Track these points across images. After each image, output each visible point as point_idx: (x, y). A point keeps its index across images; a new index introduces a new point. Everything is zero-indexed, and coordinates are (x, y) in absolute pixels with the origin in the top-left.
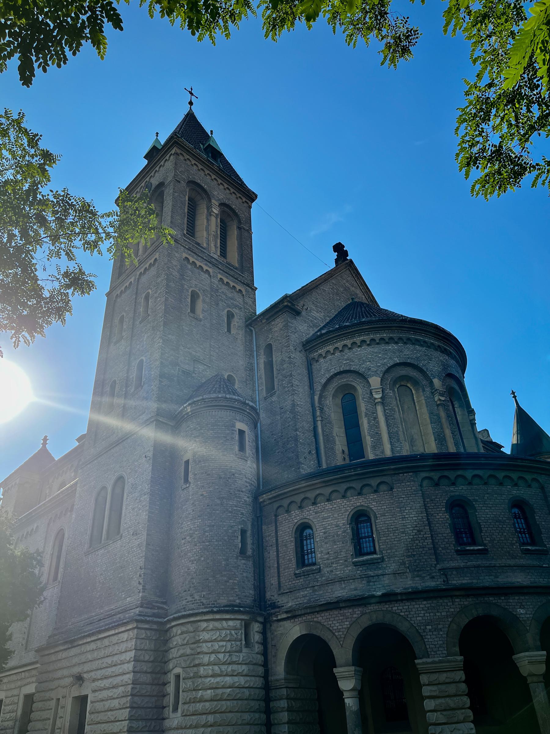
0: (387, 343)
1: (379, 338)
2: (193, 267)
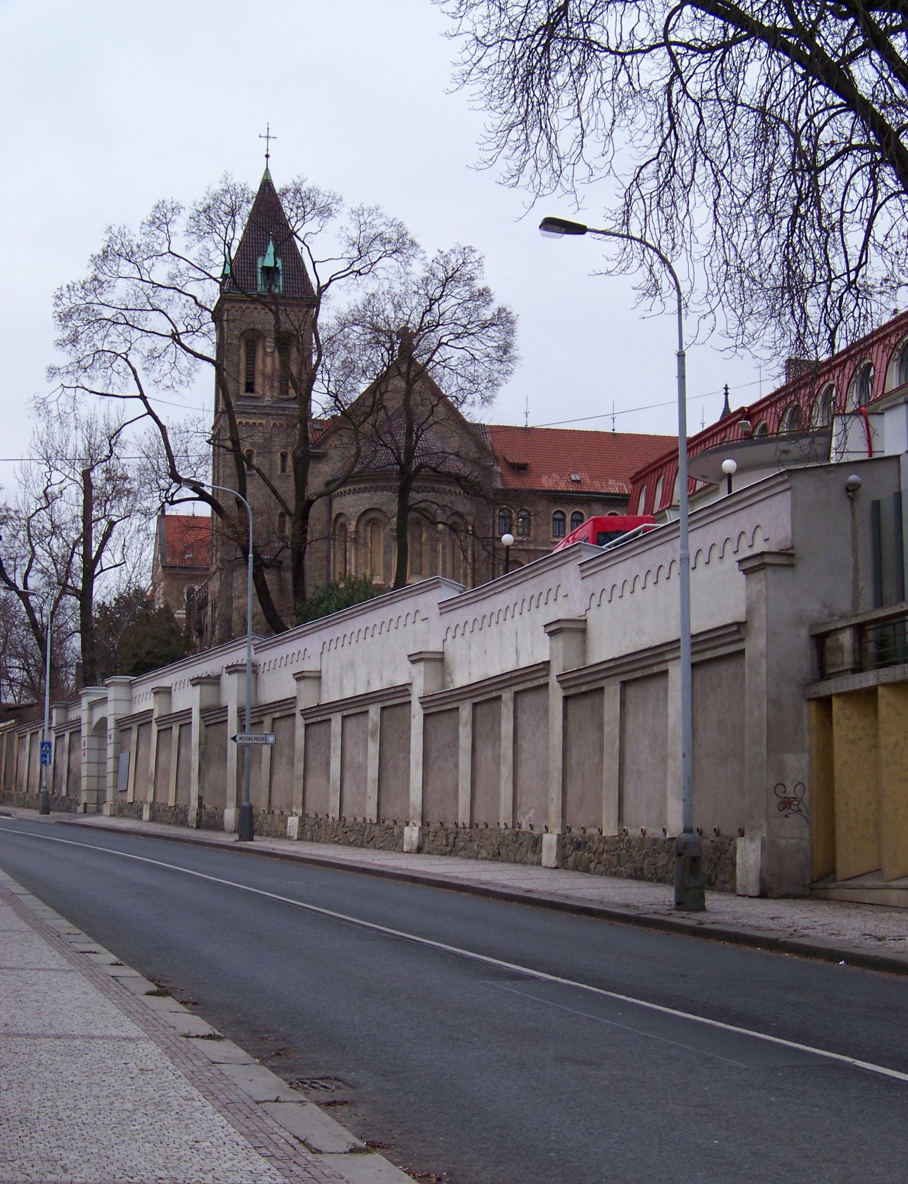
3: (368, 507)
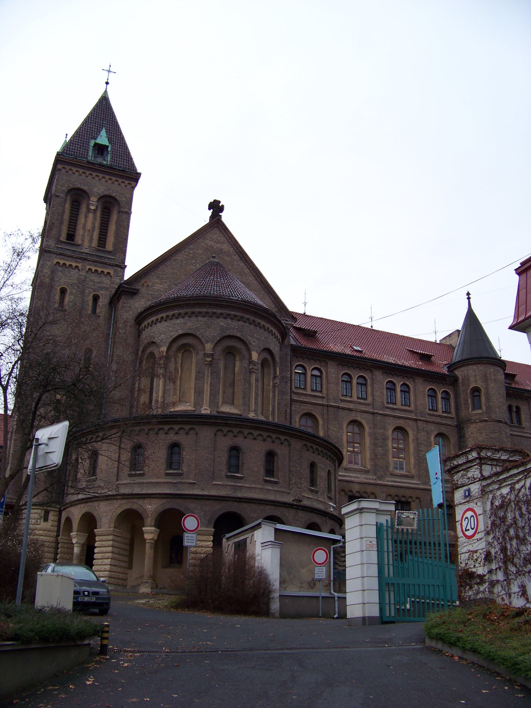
0: (177, 318)
1: (171, 314)
2: (64, 267)
3: (181, 332)
